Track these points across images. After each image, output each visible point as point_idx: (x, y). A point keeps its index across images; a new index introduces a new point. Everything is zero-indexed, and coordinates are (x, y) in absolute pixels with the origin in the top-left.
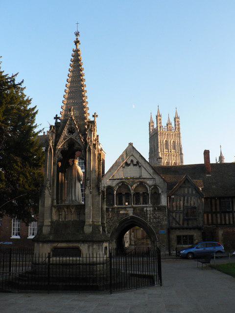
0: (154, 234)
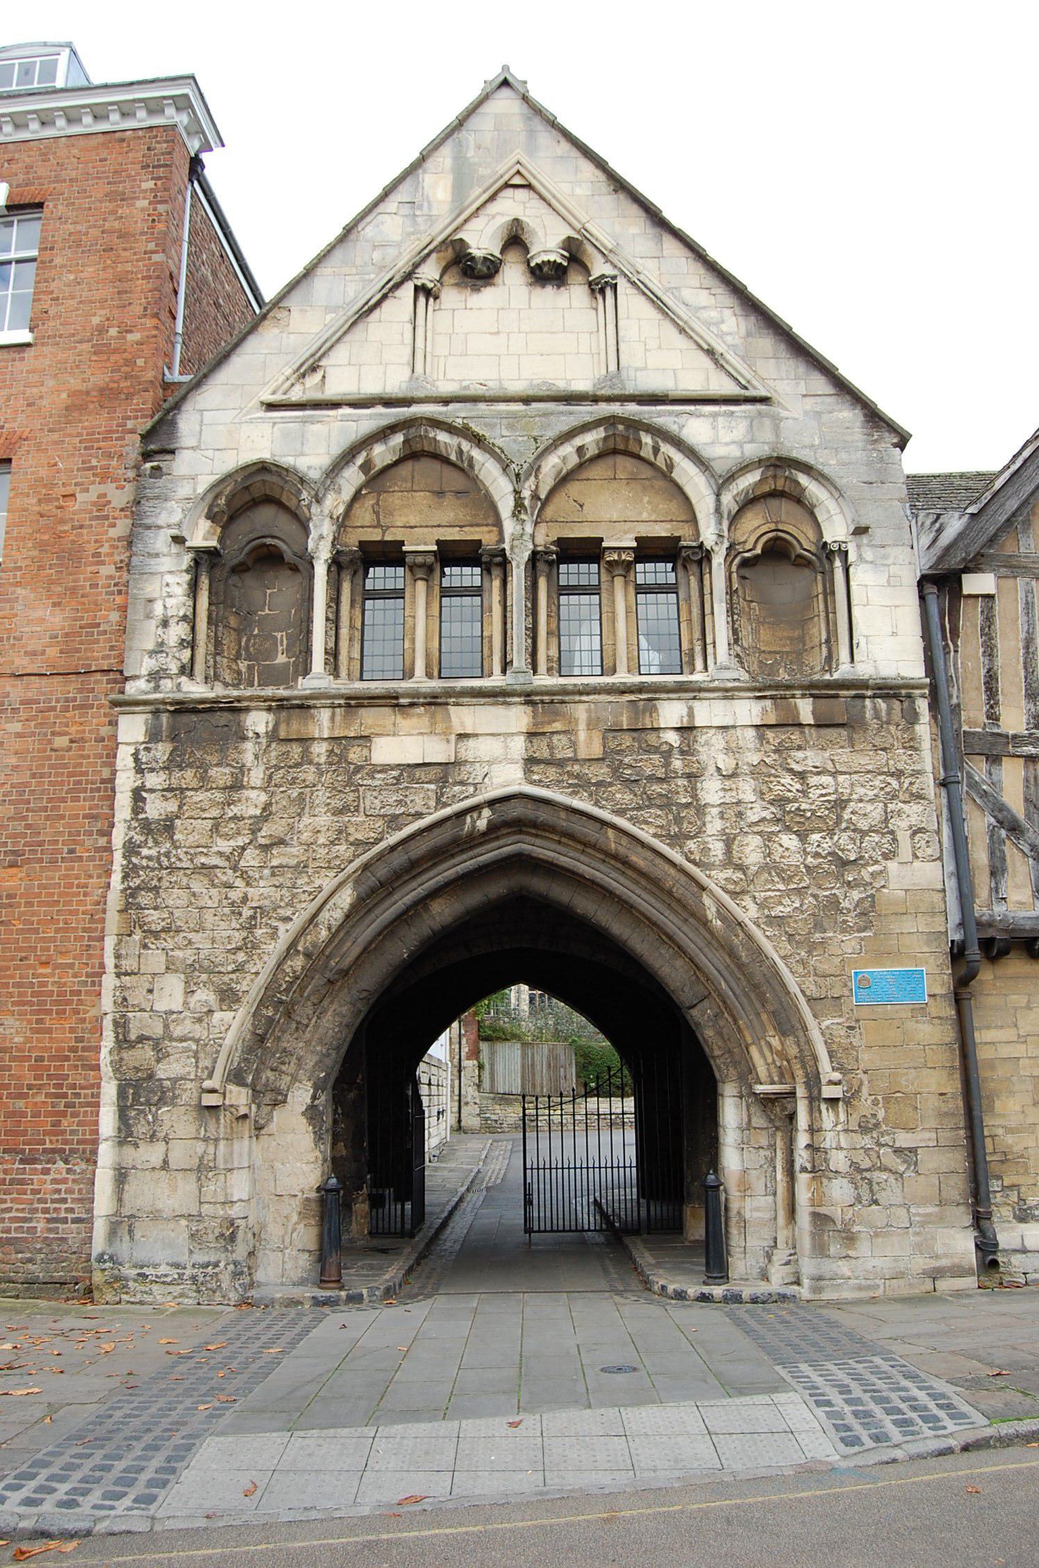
0: (788, 1023)
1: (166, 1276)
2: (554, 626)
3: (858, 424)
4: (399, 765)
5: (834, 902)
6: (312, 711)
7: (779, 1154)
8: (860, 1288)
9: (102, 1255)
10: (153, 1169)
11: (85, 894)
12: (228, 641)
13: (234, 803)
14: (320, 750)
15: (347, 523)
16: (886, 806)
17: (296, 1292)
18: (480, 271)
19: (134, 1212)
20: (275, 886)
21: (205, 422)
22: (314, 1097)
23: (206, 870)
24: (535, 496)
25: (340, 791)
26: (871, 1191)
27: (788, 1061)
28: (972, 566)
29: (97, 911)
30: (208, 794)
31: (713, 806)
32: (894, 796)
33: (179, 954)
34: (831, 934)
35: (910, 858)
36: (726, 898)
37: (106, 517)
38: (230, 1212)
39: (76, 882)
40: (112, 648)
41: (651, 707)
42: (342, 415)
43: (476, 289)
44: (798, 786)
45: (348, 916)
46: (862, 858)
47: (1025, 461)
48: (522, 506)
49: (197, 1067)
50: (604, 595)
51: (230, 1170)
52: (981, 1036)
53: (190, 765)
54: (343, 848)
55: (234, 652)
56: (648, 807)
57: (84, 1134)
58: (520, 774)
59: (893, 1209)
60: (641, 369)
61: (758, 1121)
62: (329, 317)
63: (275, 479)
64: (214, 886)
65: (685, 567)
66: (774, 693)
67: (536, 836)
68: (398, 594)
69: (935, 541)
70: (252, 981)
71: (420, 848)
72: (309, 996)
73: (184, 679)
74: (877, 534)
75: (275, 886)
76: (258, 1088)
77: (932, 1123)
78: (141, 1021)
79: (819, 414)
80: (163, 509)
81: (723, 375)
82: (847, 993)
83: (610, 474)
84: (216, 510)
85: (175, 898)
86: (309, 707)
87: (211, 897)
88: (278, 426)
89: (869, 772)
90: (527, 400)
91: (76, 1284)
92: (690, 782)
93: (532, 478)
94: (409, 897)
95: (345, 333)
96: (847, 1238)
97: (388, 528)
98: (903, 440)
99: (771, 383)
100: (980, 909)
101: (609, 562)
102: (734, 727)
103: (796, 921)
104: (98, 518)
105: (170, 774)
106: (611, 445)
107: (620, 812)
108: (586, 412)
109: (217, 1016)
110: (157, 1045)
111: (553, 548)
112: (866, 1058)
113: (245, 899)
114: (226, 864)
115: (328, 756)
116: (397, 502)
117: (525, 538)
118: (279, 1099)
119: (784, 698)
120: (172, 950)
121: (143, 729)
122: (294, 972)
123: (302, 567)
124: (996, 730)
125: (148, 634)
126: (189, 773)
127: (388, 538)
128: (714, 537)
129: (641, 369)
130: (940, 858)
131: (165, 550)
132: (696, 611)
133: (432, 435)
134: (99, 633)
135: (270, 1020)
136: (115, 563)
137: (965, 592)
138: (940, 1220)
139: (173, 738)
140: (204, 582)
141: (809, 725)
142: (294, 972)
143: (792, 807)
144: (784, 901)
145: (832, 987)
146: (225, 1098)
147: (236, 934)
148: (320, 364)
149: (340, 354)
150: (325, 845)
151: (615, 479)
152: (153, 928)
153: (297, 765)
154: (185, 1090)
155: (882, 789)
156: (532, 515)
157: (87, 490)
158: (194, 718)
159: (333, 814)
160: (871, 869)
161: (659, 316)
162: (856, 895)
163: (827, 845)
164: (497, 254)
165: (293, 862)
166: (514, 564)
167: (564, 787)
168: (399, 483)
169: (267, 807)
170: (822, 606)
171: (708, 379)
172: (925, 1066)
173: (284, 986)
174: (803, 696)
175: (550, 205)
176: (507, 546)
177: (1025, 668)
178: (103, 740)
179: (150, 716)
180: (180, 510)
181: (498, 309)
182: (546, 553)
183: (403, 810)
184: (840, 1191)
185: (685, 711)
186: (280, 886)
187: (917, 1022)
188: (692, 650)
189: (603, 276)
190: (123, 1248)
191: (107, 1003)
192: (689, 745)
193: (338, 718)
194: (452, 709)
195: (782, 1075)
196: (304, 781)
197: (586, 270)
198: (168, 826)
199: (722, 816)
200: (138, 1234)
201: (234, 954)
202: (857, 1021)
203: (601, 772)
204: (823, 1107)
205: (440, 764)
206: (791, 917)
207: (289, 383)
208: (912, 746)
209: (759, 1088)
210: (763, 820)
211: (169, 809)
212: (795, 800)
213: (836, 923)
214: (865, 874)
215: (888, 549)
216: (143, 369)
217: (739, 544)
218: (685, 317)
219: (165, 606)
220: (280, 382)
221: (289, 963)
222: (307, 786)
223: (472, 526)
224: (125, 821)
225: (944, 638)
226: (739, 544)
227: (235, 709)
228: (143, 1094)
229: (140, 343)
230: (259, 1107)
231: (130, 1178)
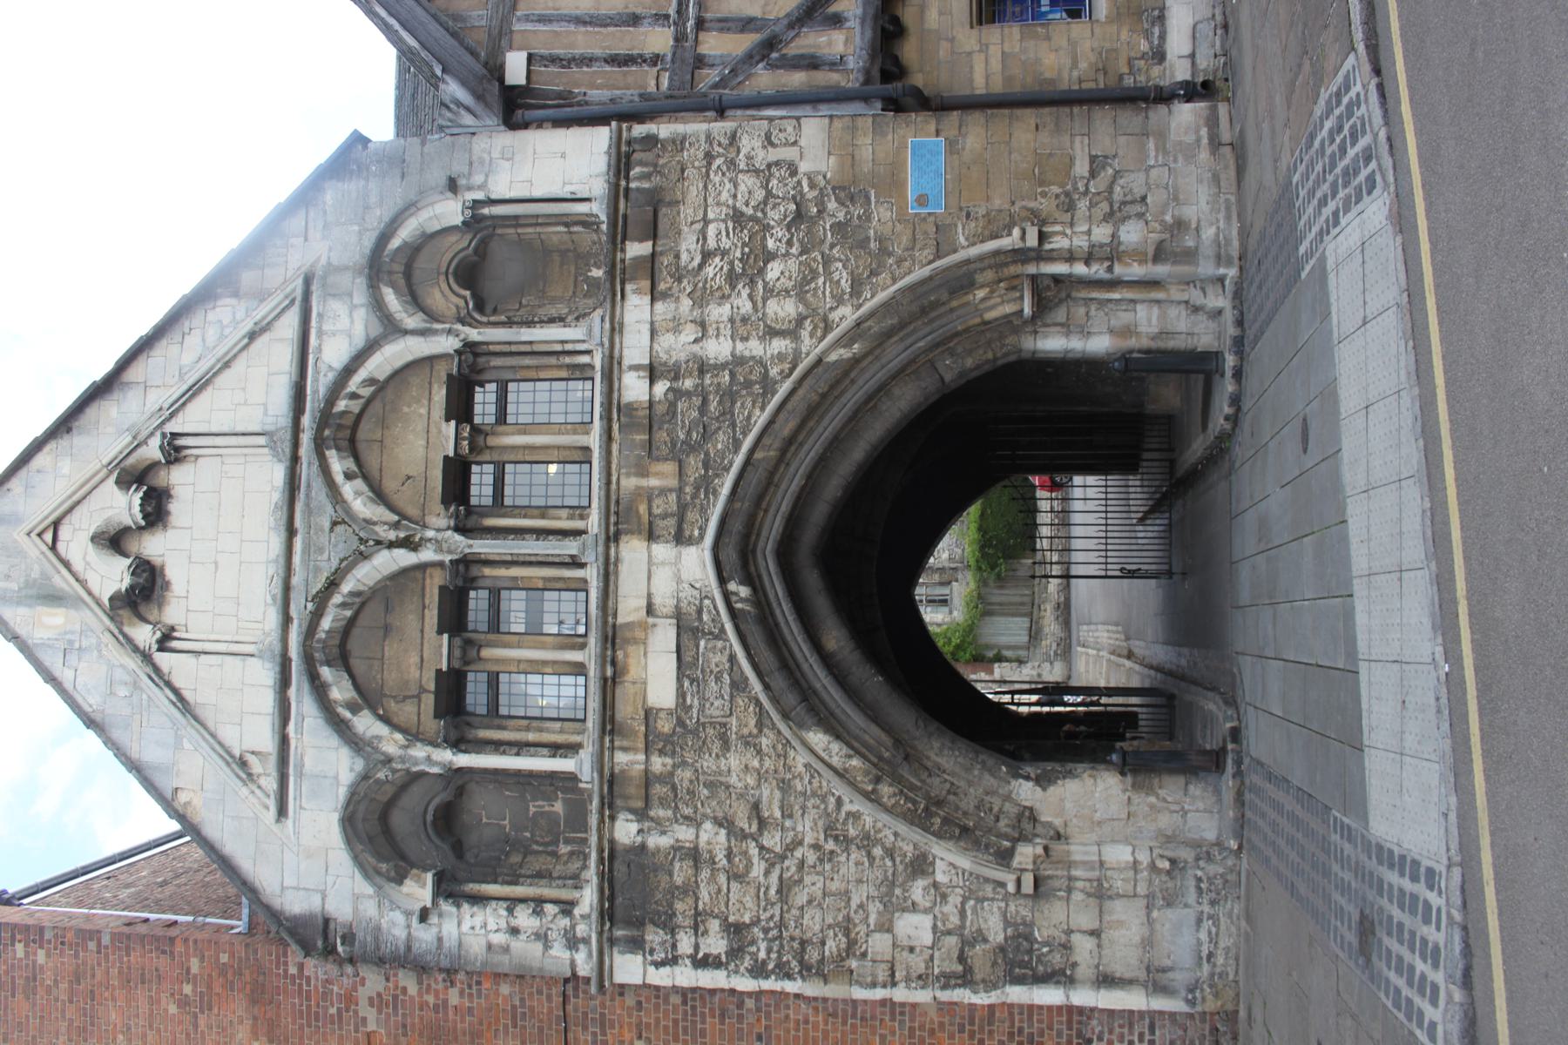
0: (960, 280)
1: (1210, 933)
2: (536, 512)
3: (340, 184)
4: (678, 678)
5: (838, 227)
6: (616, 771)
7: (1094, 295)
8: (1228, 218)
9: (1187, 1001)
10: (1099, 946)
11: (806, 1022)
12: (536, 864)
14: (659, 764)
15: (414, 731)
16: (741, 171)
17: (1228, 796)
18: (146, 580)
19: (1143, 967)
20: (803, 815)
21: (295, 884)
22: (1027, 778)
23: (784, 889)
24: (396, 526)
25: (704, 742)
26: (1132, 202)
27: (1000, 281)
28: (498, 72)
29: (825, 1009)
30: (702, 885)
31: (734, 348)
32: (732, 163)
33: (872, 920)
34: (872, 232)
35: (796, 149)
36: (830, 338)
37: (395, 997)
38: (1145, 864)
39: (793, 1032)
40: (540, 992)
41: (628, 410)
42: (296, 732)
43: (166, 585)
44: (717, 260)
45: (838, 737)
46: (794, 197)
47: (391, 14)
48: (407, 539)
49: (993, 899)
50: (505, 458)
52: (979, 86)
53: (671, 905)
54: (764, 742)
55: (549, 858)
56: (733, 415)
57: (1061, 1023)
59: (1151, 181)
60: (266, 410)
61: (1060, 315)
62: (186, 745)
63: (362, 808)
64: (801, 881)
65: (480, 371)
66: (618, 280)
67: (758, 535)
69: (468, 109)
70: (903, 840)
71: (767, 658)
72: (923, 781)
73: (577, 912)
74: (458, 168)
75: (803, 815)
76: (1016, 835)
77: (1067, 138)
78: (943, 960)
79: (326, 226)
80: (389, 932)
81: (278, 324)
82: (932, 219)
83: (376, 446)
84: (393, 874)
85: (813, 922)
86: (612, 775)
87: (813, 884)
88: (304, 805)
89: (705, 187)
90: (291, 532)
91: (1217, 1030)
92: (708, 372)
93: (377, 528)
94: (818, 672)
95: (206, 728)
96: (1179, 229)
97: (421, 686)
98: (358, 140)
99: (289, 274)
100: (850, 80)
101: (472, 449)
102: (652, 323)
103: (857, 267)
104: (395, 1008)
105: (679, 927)
106: (345, 444)
107: (737, 445)
108: (309, 468)
109: (941, 877)
110: (967, 943)
111: (452, 508)
112: (997, 203)
113: (816, 847)
114: (778, 867)
115: (666, 755)
116: (393, 675)
117: (440, 538)
118: (1029, 815)
119: (624, 271)
120: (868, 926)
121: (629, 956)
122: (895, 795)
123: (459, 779)
124: (669, 58)
125: (527, 951)
126: (679, 906)
127: (432, 686)
128: (451, 338)
129: (266, 410)
131: (434, 930)
132: (527, 361)
133: (323, 636)
134: (523, 1006)
135: (946, 821)
136: (446, 988)
137: (523, 81)
138: (1162, 136)
139: (640, 924)
141: (654, 246)
142: (895, 795)
144: (836, 279)
145: (926, 233)
146: (1026, 870)
147: (853, 856)
148: (238, 755)
149: (230, 736)
150: (761, 760)
152: (843, 946)
153: (674, 788)
154: (1017, 912)
155: (724, 174)
156: (415, 529)
157: (364, 1020)
158: (619, 900)
159: (728, 750)
160: (806, 189)
161: (210, 389)
162: (832, 205)
163: (779, 232)
164: (128, 561)
165: (778, 794)
166: (467, 551)
167: (708, 502)
168: (374, 673)
169: (719, 823)
170: (530, 230)
171: (281, 340)
172: (1008, 143)
173: (910, 805)
174: (623, 250)
175: (78, 502)
176: (447, 558)
177: (606, 26)
178: (639, 1003)
179: (615, 950)
180: (391, 913)
182: (457, 517)
183: (726, 676)
184: (1131, 234)
185: (633, 374)
186: (804, 808)
187: (963, 149)
189: (161, 448)
190: (1180, 978)
191: (922, 996)
192: (669, 371)
193: (625, 743)
194: (621, 620)
195: (1014, 288)
196: (691, 781)
197: (153, 466)
198: (736, 931)
199: (745, 339)
200: (1167, 963)
201: (874, 859)
202: (961, 209)
203: (694, 464)
204: (1047, 247)
205: (678, 635)
206: (852, 272)
207: (257, 791)
208: (679, 143)
209: (1027, 311)
210: (751, 297)
211: (717, 928)
212: (731, 263)
213: (860, 226)
214: (812, 195)
215: (474, 158)
216: (232, 955)
217: (459, 312)
218: (213, 361)
219: (496, 931)
220: (254, 800)
221: (885, 800)
222: (697, 779)
223: (423, 596)
224: (728, 976)
226: (459, 312)
227: (611, 854)
228: (1019, 957)
229: (202, 959)
230: (1037, 835)
231: (1109, 970)
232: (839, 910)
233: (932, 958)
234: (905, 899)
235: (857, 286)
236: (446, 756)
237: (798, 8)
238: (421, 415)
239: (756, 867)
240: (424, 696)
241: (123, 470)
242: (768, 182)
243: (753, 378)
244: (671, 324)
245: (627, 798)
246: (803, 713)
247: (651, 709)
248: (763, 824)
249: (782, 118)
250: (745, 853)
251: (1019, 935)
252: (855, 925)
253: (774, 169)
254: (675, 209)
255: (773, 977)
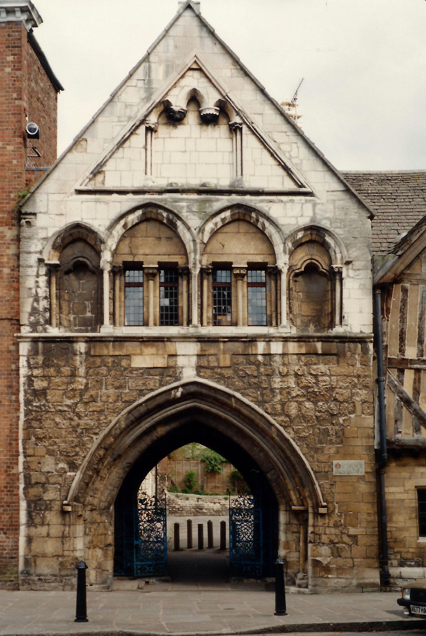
5: (326, 432)
10: (43, 537)
13: (72, 383)
16: (351, 391)
18: (177, 117)
19: (36, 554)
20: (90, 419)
21: (50, 199)
32: (355, 386)
44: (314, 381)
46: (340, 413)
51: (75, 537)
53: (53, 366)
58: (195, 372)
65: (270, 276)
68: (140, 285)
83: (236, 230)
87: (64, 423)
92: (267, 378)
107: (237, 390)
110: (43, 485)
111: (210, 267)
115: (112, 363)
116: (141, 242)
126: (52, 370)
127: (136, 260)
130: (373, 414)
140: (54, 280)
142: (100, 456)
143: (310, 390)
151: (239, 232)
152: (40, 436)
153: (99, 367)
155: (350, 383)
163: (325, 407)
165: (98, 409)
166: (193, 275)
169: (87, 384)
181: (186, 138)
188: (271, 315)
189: (236, 123)
196: (102, 374)
197: (228, 118)
198: (43, 392)
210: (298, 395)
214: (341, 420)
223: (174, 255)
225: (383, 314)
231: (34, 540)
232: (54, 435)
233: (37, 471)
234: (59, 460)
235: (303, 439)
236: (107, 268)
237: (423, 413)
238: (250, 251)
239: (69, 401)
240: (132, 256)
241: (226, 102)
242: (347, 402)
243: (265, 397)
244: (286, 362)
245: (94, 347)
246: (131, 419)
247: (131, 358)
248: (86, 403)
249: (374, 407)
250: (74, 396)
251: (47, 505)
252: (48, 441)
253: (352, 405)
254: (335, 362)
255: (26, 409)
